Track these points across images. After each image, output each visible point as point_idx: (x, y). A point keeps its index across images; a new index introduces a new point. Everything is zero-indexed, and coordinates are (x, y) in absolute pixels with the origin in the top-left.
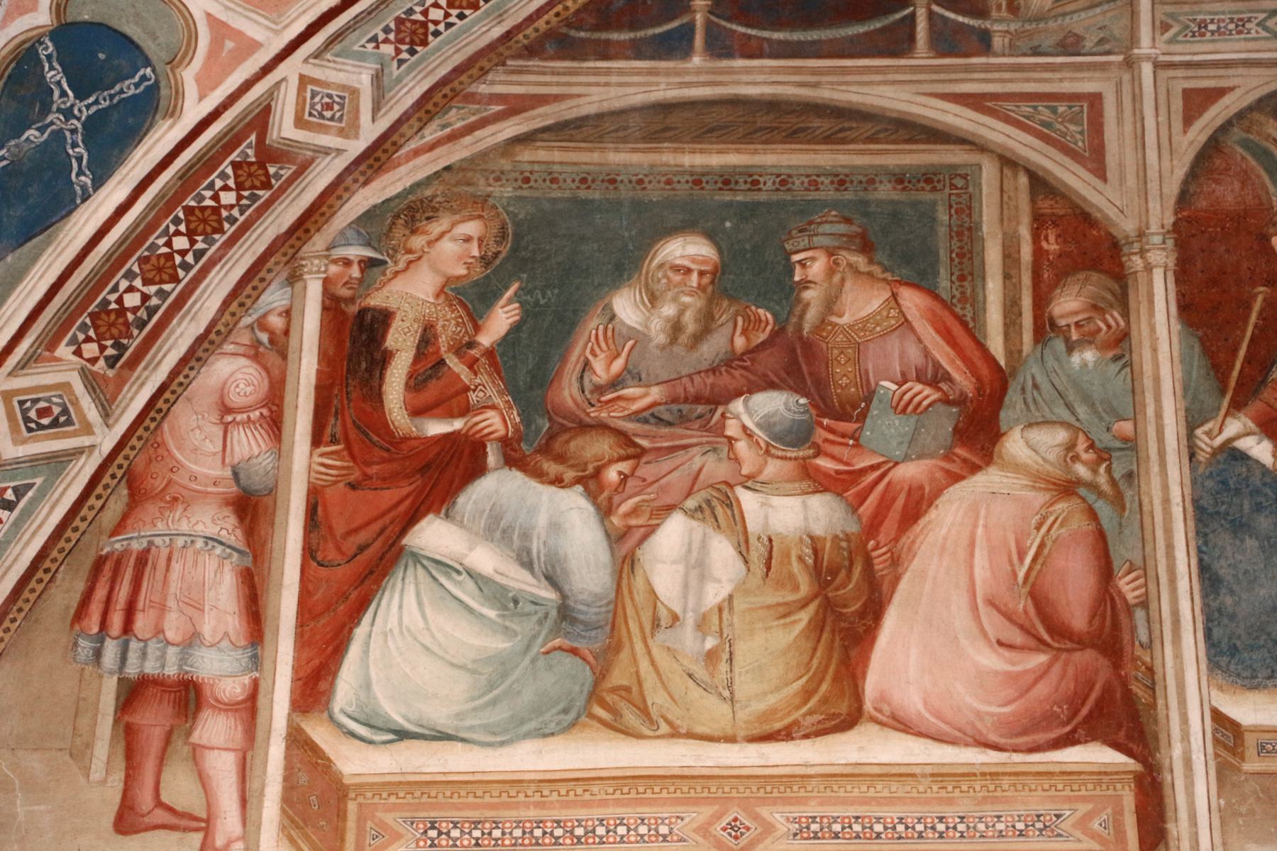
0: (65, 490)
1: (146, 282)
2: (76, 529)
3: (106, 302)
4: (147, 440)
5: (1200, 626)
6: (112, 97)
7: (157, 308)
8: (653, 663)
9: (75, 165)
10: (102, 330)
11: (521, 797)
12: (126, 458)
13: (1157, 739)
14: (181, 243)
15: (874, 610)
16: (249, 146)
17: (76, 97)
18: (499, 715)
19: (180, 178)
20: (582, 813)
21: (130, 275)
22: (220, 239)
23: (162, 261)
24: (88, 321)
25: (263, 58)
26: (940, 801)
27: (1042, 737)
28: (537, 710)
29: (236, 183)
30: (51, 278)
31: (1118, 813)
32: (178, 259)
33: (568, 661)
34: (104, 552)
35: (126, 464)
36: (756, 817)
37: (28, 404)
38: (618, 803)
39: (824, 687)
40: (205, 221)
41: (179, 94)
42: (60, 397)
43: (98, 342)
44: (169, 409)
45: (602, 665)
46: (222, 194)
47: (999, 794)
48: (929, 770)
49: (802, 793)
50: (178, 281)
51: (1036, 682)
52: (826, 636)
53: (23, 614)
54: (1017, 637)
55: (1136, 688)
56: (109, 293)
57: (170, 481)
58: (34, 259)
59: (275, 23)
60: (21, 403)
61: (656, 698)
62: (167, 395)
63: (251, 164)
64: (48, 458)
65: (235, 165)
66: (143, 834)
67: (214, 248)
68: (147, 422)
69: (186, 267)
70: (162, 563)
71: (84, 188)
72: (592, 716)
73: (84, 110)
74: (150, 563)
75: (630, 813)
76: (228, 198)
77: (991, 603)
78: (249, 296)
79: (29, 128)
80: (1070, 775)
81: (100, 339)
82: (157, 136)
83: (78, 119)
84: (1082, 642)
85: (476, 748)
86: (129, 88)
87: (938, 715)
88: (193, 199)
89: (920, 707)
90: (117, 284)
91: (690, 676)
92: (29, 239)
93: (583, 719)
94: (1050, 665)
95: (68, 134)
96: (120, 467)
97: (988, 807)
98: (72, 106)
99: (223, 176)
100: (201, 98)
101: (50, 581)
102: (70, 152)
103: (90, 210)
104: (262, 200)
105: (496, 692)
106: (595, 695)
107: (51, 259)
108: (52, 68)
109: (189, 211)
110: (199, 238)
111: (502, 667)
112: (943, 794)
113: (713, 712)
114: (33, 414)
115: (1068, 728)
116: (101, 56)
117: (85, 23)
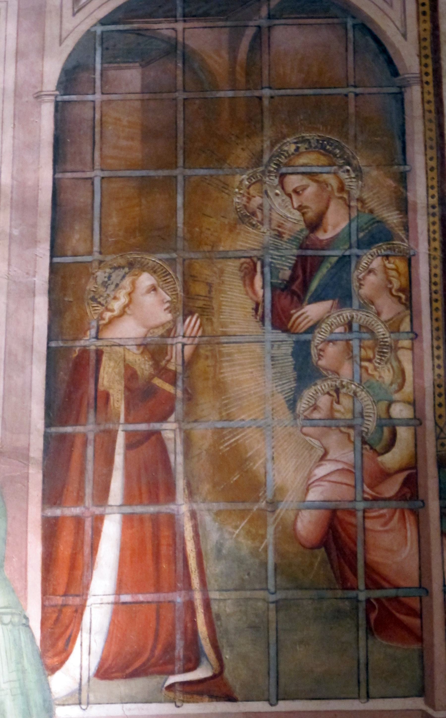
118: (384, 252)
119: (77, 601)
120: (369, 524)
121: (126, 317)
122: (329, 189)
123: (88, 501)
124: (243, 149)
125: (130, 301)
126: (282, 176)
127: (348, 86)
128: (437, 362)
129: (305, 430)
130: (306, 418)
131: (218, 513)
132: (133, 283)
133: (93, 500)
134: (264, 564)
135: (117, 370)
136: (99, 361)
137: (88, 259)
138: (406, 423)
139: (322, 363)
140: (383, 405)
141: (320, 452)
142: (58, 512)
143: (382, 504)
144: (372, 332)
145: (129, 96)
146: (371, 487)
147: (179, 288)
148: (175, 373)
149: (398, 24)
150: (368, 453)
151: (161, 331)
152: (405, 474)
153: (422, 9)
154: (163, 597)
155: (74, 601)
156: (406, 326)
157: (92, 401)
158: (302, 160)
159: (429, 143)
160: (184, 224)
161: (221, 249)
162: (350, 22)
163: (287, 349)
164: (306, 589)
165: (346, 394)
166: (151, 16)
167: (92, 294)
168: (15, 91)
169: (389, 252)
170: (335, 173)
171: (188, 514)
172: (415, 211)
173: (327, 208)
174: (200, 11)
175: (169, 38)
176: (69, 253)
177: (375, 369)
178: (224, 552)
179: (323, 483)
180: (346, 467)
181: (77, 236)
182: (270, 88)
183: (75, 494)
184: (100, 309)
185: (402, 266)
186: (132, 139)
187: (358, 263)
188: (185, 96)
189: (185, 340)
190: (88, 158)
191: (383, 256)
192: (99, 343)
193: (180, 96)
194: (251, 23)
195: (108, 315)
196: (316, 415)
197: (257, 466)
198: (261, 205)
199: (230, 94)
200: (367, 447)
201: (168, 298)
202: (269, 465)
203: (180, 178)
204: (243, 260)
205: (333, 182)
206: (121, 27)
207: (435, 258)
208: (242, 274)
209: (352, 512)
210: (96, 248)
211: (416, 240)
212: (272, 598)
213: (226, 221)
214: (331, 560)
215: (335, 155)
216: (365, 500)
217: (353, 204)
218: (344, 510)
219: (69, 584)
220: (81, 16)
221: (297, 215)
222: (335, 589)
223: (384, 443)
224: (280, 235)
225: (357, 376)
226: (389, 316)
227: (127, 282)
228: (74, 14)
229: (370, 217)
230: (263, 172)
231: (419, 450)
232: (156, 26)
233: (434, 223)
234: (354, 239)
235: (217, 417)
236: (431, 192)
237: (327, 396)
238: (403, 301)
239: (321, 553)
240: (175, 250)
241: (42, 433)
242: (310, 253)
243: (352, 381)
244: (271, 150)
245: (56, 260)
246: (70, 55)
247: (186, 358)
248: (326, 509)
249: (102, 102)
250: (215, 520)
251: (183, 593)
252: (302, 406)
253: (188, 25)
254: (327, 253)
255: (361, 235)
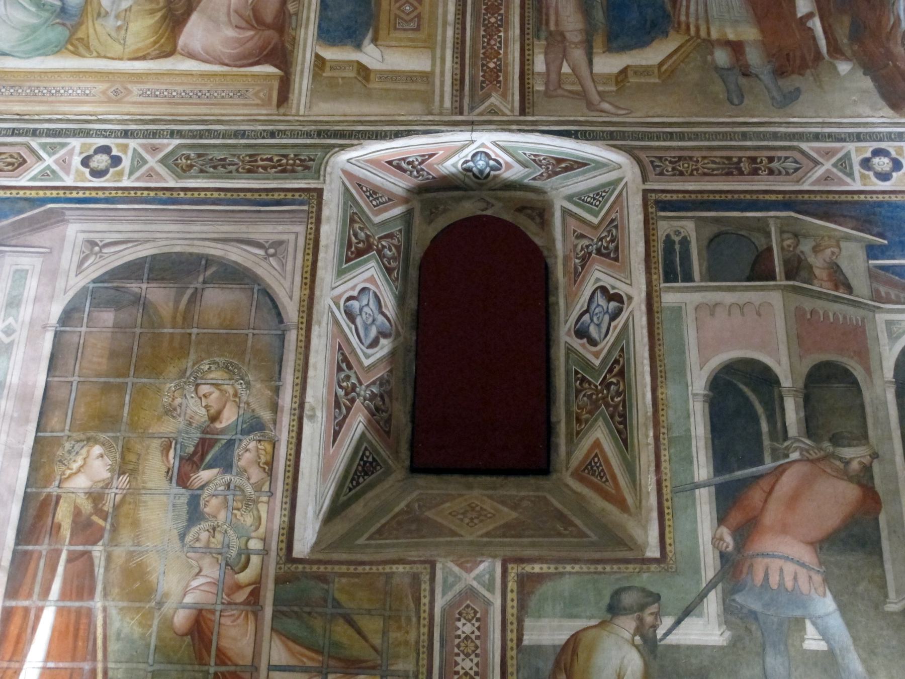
5: (317, 23)
8: (95, 30)
11: (32, 78)
13: (291, 63)
15: (189, 11)
18: (28, 47)
20: (55, 85)
26: (201, 84)
27: (245, 62)
28: (45, 46)
31: (271, 89)
33: (60, 28)
36: (126, 89)
38: (70, 81)
39: (163, 40)
45: (75, 29)
47: (225, 82)
48: (199, 73)
49: (146, 80)
51: (248, 41)
52: (167, 21)
54: (244, 24)
55: (288, 46)
61: (93, 42)
72: (67, 49)
75: (75, 85)
77: (236, 12)
80: (253, 76)
84: (269, 27)
85: (17, 59)
87: (207, 53)
89: (200, 49)
91: (109, 35)
93: (63, 50)
94: (255, 35)
97: (220, 87)
105: (29, 38)
106: (69, 41)
111: (34, 29)
112: (203, 82)
113: (118, 49)
115: (257, 59)
118: (258, 438)
119: (17, 665)
120: (223, 620)
121: (80, 474)
122: (227, 395)
123: (35, 597)
124: (174, 367)
125: (84, 464)
126: (197, 385)
127: (249, 329)
128: (284, 512)
129: (189, 554)
130: (191, 547)
131: (121, 609)
132: (88, 452)
133: (39, 595)
134: (148, 646)
135: (69, 509)
136: (57, 503)
137: (61, 434)
138: (257, 552)
139: (207, 510)
140: (243, 540)
141: (197, 570)
142: (13, 603)
143: (233, 607)
144: (243, 491)
145: (104, 330)
146: (228, 595)
147: (118, 456)
148: (107, 513)
149: (288, 290)
150: (229, 571)
151: (101, 485)
152: (253, 586)
153: (304, 281)
154: (75, 665)
155: (14, 665)
156: (266, 488)
157: (49, 529)
158: (212, 375)
159: (297, 367)
160: (128, 414)
161: (150, 431)
162: (256, 288)
163: (184, 500)
164: (174, 663)
165: (220, 532)
166: (128, 278)
167: (60, 458)
168: (30, 323)
169: (261, 438)
170: (232, 385)
171: (101, 609)
172: (282, 411)
173: (224, 407)
174: (159, 277)
175: (136, 293)
176: (49, 430)
177: (242, 515)
178: (122, 636)
179: (195, 591)
180: (212, 580)
181: (56, 419)
182: (197, 328)
183: (27, 592)
184: (64, 467)
185: (269, 448)
186: (102, 357)
187: (240, 444)
188: (141, 330)
189: (117, 491)
190: (72, 368)
191: (257, 440)
192: (59, 491)
193: (138, 330)
194: (192, 286)
195: (68, 472)
196: (197, 545)
197: (153, 578)
198: (181, 404)
199: (171, 331)
200: (229, 568)
201: (110, 463)
202: (161, 578)
203: (130, 385)
204: (163, 439)
205: (231, 391)
206: (106, 285)
207: (291, 443)
208: (162, 449)
209: (213, 612)
210: (67, 428)
211: (281, 431)
212: (150, 669)
213: (156, 413)
214: (194, 645)
215: (234, 373)
216: (223, 603)
217: (242, 405)
218: (206, 610)
219: (14, 653)
220: (80, 277)
221: (203, 411)
222: (194, 664)
223: (240, 565)
224: (190, 424)
225: (229, 520)
226: (256, 481)
227: (84, 451)
228: (76, 276)
229: (252, 414)
230: (185, 382)
231: (264, 572)
232: (128, 285)
233: (294, 420)
234: (239, 428)
235: (130, 543)
236: (294, 400)
237: (207, 533)
238: (267, 470)
239: (188, 639)
240: (120, 431)
241: (12, 549)
242: (208, 436)
243: (225, 523)
244: (192, 368)
245: (40, 434)
246: (69, 302)
247: (116, 503)
248: (195, 609)
249: (86, 332)
250: (119, 614)
251: (90, 663)
252: (189, 538)
253: (150, 285)
254: (220, 437)
255: (245, 426)
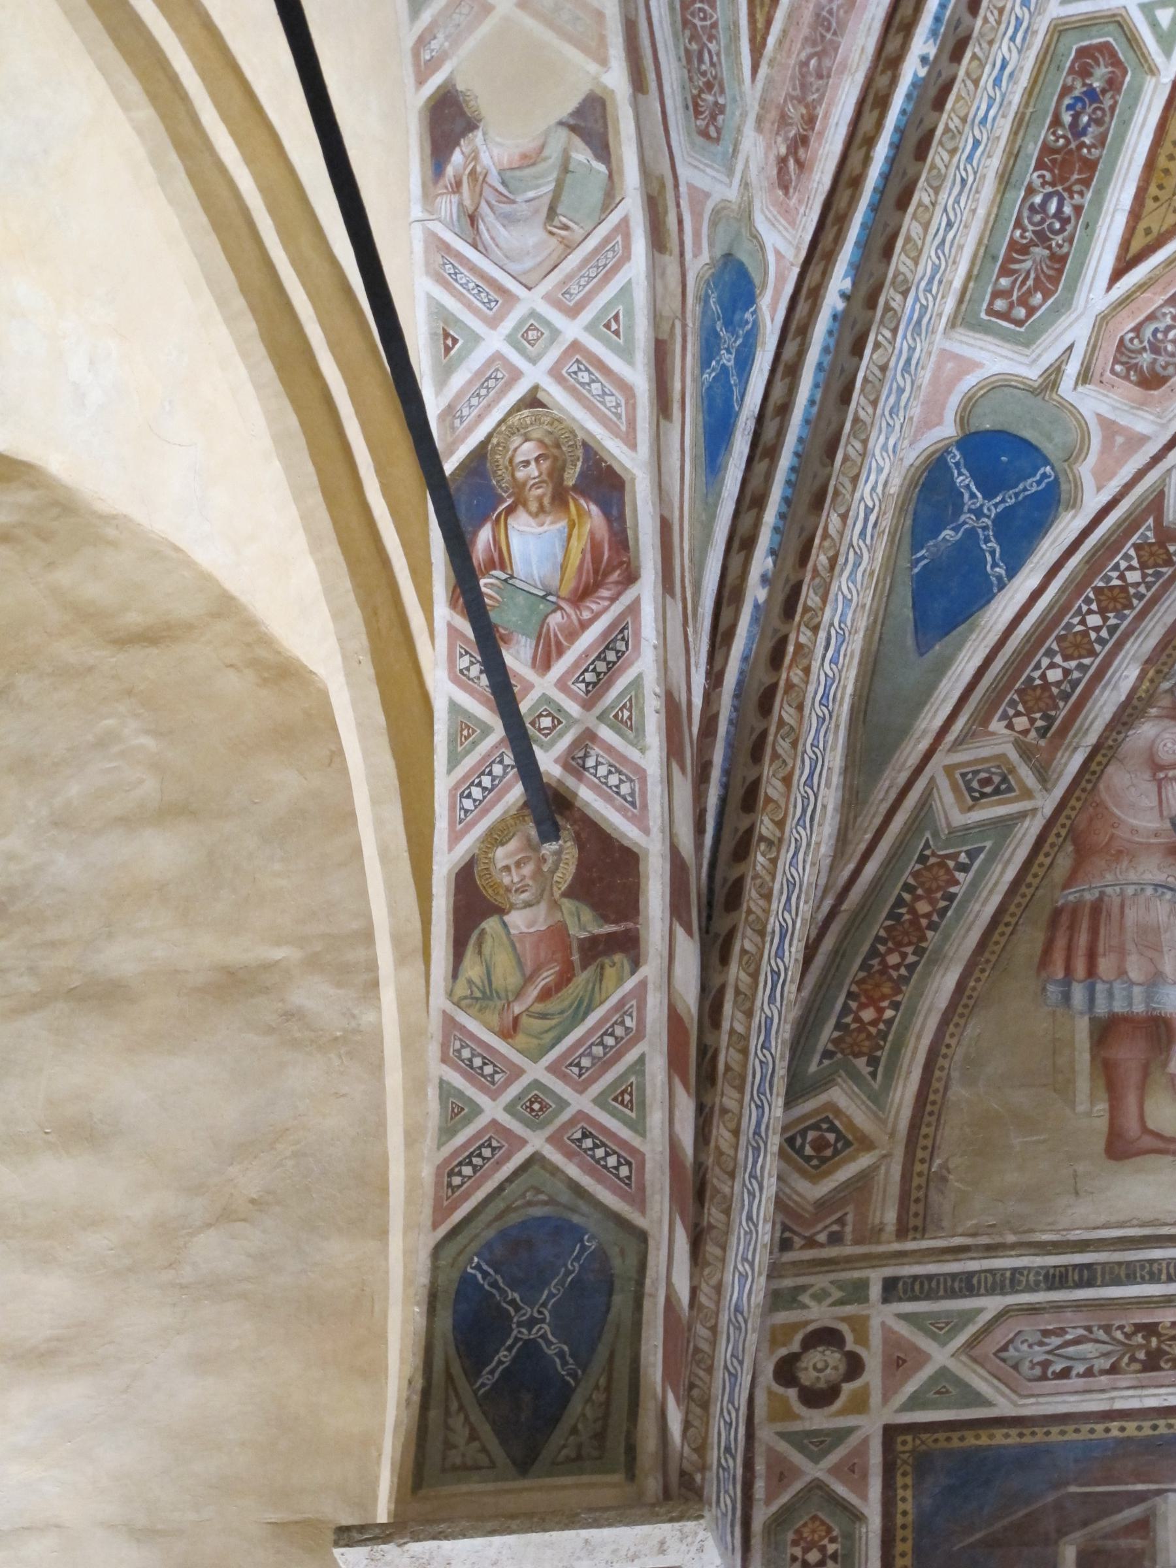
0: (1015, 850)
1: (1066, 658)
2: (1029, 886)
3: (1030, 679)
4: (1086, 800)
6: (1017, 495)
7: (1079, 681)
9: (989, 558)
10: (1030, 704)
12: (1068, 817)
14: (1094, 620)
16: (1148, 528)
17: (984, 498)
19: (1087, 562)
21: (1050, 653)
22: (1131, 614)
23: (1079, 638)
24: (1016, 697)
25: (1153, 448)
29: (1139, 562)
30: (977, 661)
32: (1093, 635)
34: (1059, 904)
35: (1068, 823)
37: (970, 776)
40: (1115, 599)
41: (1078, 485)
42: (998, 767)
43: (1027, 715)
44: (1102, 771)
46: (1127, 574)
50: (1096, 655)
53: (991, 965)
56: (1033, 670)
57: (1112, 837)
58: (959, 647)
59: (1160, 417)
60: (963, 775)
62: (1099, 758)
63: (1151, 544)
64: (994, 823)
65: (1137, 547)
66: (1133, 1159)
67: (1126, 623)
68: (1083, 784)
69: (1102, 642)
70: (1115, 910)
71: (999, 578)
73: (992, 508)
74: (1104, 914)
76: (1133, 577)
78: (1164, 664)
79: (945, 529)
81: (1029, 712)
82: (1061, 526)
83: (988, 517)
86: (1031, 486)
88: (1101, 580)
90: (1039, 662)
92: (954, 628)
95: (980, 531)
96: (1063, 826)
98: (982, 506)
99: (1127, 557)
100: (1099, 489)
101: (1012, 933)
102: (984, 547)
103: (1007, 598)
104: (1166, 576)
107: (976, 643)
108: (960, 474)
109: (1097, 590)
110: (1111, 615)
114: (975, 785)
116: (1003, 458)
117: (987, 431)
